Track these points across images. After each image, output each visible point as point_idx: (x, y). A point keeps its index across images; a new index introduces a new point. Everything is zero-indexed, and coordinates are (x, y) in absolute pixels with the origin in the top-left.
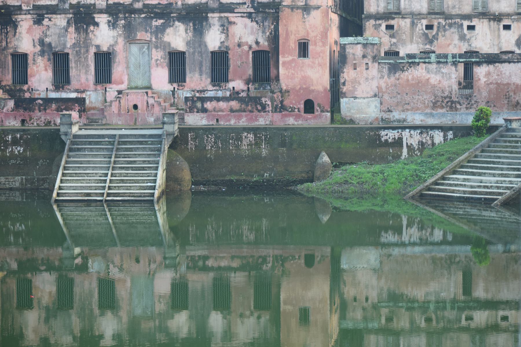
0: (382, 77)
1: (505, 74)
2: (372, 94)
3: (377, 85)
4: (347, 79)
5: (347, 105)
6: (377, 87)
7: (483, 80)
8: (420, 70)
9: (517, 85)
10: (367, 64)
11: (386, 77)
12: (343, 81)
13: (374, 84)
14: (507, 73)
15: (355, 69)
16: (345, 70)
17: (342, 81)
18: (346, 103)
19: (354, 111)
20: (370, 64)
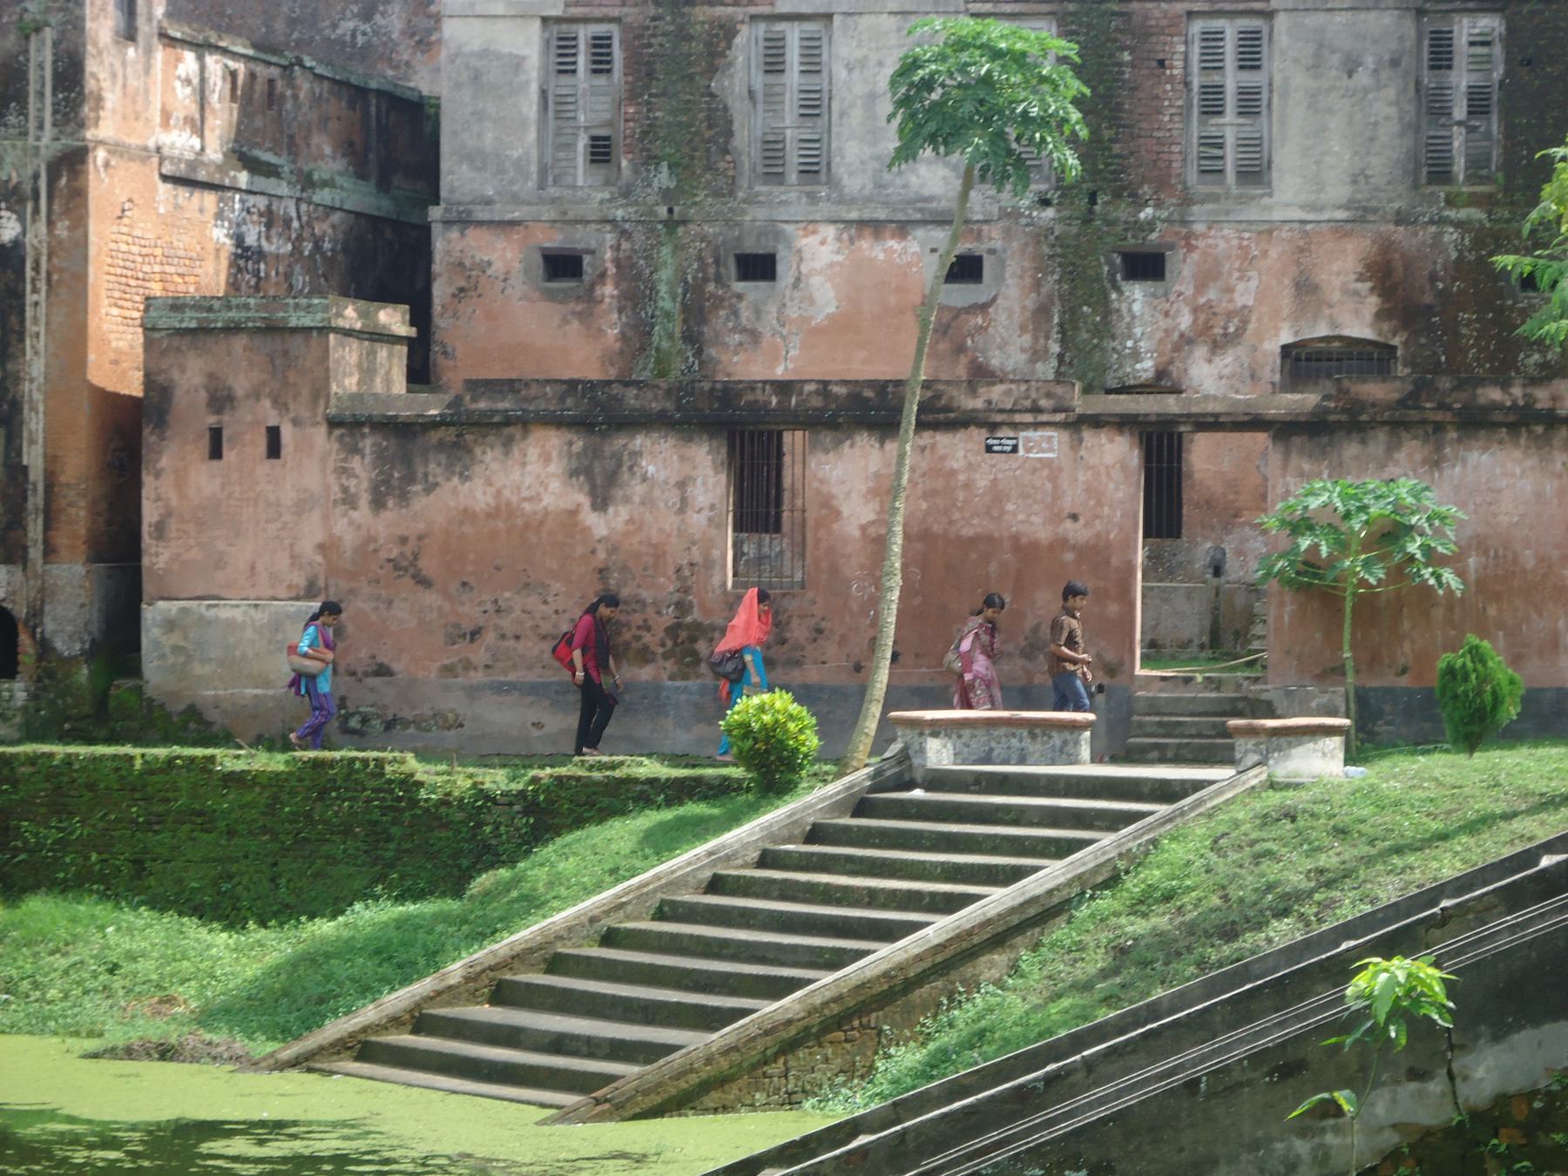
0: (349, 500)
1: (967, 486)
2: (299, 579)
3: (319, 537)
4: (174, 503)
5: (176, 638)
6: (321, 548)
7: (857, 512)
8: (535, 467)
9: (1034, 546)
10: (274, 435)
11: (364, 499)
12: (155, 519)
13: (311, 534)
14: (982, 483)
15: (216, 453)
16: (164, 462)
17: (150, 513)
18: (170, 625)
19: (207, 669)
20: (287, 433)
